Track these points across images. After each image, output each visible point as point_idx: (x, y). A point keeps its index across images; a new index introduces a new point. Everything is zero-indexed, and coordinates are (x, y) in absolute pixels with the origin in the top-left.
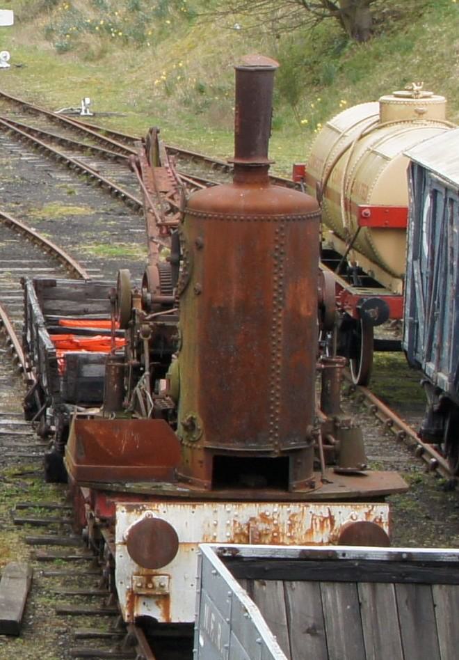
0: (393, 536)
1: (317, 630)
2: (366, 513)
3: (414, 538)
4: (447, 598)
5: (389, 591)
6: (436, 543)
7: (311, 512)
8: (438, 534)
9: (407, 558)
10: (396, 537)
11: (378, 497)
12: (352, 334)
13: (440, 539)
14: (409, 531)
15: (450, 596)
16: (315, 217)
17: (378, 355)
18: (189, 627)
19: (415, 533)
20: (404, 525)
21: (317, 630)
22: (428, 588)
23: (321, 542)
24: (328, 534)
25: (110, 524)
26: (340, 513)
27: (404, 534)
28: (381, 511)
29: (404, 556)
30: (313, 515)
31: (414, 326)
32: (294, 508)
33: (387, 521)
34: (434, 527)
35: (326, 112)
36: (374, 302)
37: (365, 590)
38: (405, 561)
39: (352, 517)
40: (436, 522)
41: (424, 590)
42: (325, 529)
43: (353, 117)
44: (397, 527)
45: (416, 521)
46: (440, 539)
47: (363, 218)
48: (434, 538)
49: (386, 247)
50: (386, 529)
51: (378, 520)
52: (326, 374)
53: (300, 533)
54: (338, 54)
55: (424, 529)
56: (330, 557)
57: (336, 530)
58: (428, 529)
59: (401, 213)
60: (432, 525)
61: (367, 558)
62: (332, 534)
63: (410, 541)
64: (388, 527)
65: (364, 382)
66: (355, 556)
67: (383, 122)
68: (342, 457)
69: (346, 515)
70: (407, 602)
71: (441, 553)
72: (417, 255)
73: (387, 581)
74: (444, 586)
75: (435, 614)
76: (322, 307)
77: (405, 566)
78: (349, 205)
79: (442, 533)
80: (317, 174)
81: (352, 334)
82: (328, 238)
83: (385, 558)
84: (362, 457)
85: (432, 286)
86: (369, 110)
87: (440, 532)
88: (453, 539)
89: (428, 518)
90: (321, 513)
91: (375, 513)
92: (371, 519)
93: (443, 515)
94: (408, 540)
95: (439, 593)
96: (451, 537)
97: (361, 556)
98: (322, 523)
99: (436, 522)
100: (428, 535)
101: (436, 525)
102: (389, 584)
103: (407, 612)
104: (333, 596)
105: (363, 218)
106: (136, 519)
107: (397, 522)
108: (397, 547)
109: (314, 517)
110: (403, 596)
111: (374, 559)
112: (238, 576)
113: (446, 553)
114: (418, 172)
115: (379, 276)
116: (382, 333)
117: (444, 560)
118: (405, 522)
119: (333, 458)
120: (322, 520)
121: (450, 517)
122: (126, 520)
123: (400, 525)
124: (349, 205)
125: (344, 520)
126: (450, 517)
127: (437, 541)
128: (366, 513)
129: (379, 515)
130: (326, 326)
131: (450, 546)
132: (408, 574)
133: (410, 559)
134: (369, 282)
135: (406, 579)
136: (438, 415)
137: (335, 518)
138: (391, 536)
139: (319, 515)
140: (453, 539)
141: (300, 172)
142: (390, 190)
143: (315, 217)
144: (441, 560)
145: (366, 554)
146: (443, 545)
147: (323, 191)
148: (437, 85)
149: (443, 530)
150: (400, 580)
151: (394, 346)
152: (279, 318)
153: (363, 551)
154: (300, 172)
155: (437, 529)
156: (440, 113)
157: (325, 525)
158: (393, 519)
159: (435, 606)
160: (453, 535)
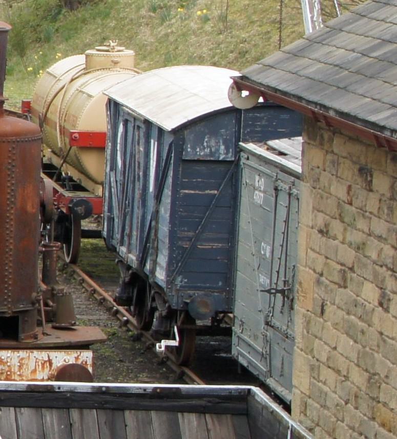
0: (96, 374)
2: (75, 358)
3: (111, 376)
4: (135, 420)
5: (92, 415)
6: (127, 380)
7: (35, 357)
8: (129, 373)
9: (106, 391)
10: (97, 375)
11: (84, 346)
12: (65, 226)
13: (130, 376)
14: (107, 371)
15: (137, 418)
16: (38, 139)
17: (85, 241)
19: (111, 372)
20: (104, 366)
22: (121, 413)
23: (42, 379)
24: (47, 373)
26: (56, 357)
27: (103, 373)
28: (87, 356)
29: (104, 389)
30: (37, 359)
31: (111, 220)
32: (22, 354)
33: (91, 363)
34: (125, 367)
35: (46, 63)
36: (82, 202)
37: (75, 414)
38: (104, 393)
39: (65, 361)
40: (127, 364)
41: (118, 414)
42: (45, 369)
43: (66, 66)
44: (98, 368)
45: (112, 363)
46: (130, 376)
47: (73, 140)
48: (126, 376)
49: (91, 162)
50: (90, 369)
51: (84, 363)
52: (46, 255)
53: (27, 372)
54: (54, 19)
55: (118, 369)
56: (49, 390)
57: (53, 370)
58: (121, 369)
59: (103, 135)
60: (124, 366)
61: (76, 391)
62: (50, 373)
63: (108, 378)
64: (91, 368)
65: (74, 261)
66: (67, 389)
67: (88, 69)
68: (57, 316)
69: (61, 359)
70: (105, 423)
71: (131, 387)
72: (113, 167)
73: (91, 408)
74: (133, 411)
75: (126, 431)
76: (43, 206)
77: (104, 397)
78: (63, 131)
79: (131, 373)
80: (39, 108)
81: (65, 226)
82: (47, 155)
83: (90, 391)
84: (72, 316)
85: (124, 191)
86: (78, 60)
87: (130, 371)
88: (139, 376)
89: (121, 361)
90: (42, 357)
91: (82, 357)
92: (79, 362)
93: (132, 359)
94: (107, 377)
95: (129, 417)
96: (138, 375)
97: (72, 389)
98: (43, 365)
99: (127, 364)
100: (121, 374)
101: (127, 367)
102: (92, 410)
103: (106, 430)
104: (51, 418)
105: (73, 140)
107: (98, 364)
108: (98, 382)
109: (37, 361)
110: (103, 418)
111: (82, 391)
113: (135, 387)
114: (114, 106)
115: (85, 183)
116: (87, 224)
117: (133, 392)
118: (105, 364)
119: (51, 317)
120: (43, 362)
121: (137, 360)
123: (101, 367)
124: (63, 131)
125: (59, 363)
126: (137, 360)
127: (128, 378)
128: (75, 358)
129: (85, 358)
130: (46, 220)
131: (137, 382)
132: (106, 402)
133: (108, 391)
134: (78, 187)
135: (105, 406)
136: (128, 285)
137: (53, 361)
138: (94, 374)
139: (41, 359)
140: (139, 376)
141: (27, 106)
142: (93, 119)
143: (38, 139)
144: (130, 392)
145: (75, 387)
146: (132, 381)
147: (44, 120)
148: (128, 42)
149: (132, 370)
150: (100, 407)
151: (96, 234)
152: (12, 214)
153: (74, 386)
154: (27, 106)
155: (128, 369)
156: (130, 62)
157: (45, 367)
158: (95, 362)
159: (126, 426)
160: (139, 373)
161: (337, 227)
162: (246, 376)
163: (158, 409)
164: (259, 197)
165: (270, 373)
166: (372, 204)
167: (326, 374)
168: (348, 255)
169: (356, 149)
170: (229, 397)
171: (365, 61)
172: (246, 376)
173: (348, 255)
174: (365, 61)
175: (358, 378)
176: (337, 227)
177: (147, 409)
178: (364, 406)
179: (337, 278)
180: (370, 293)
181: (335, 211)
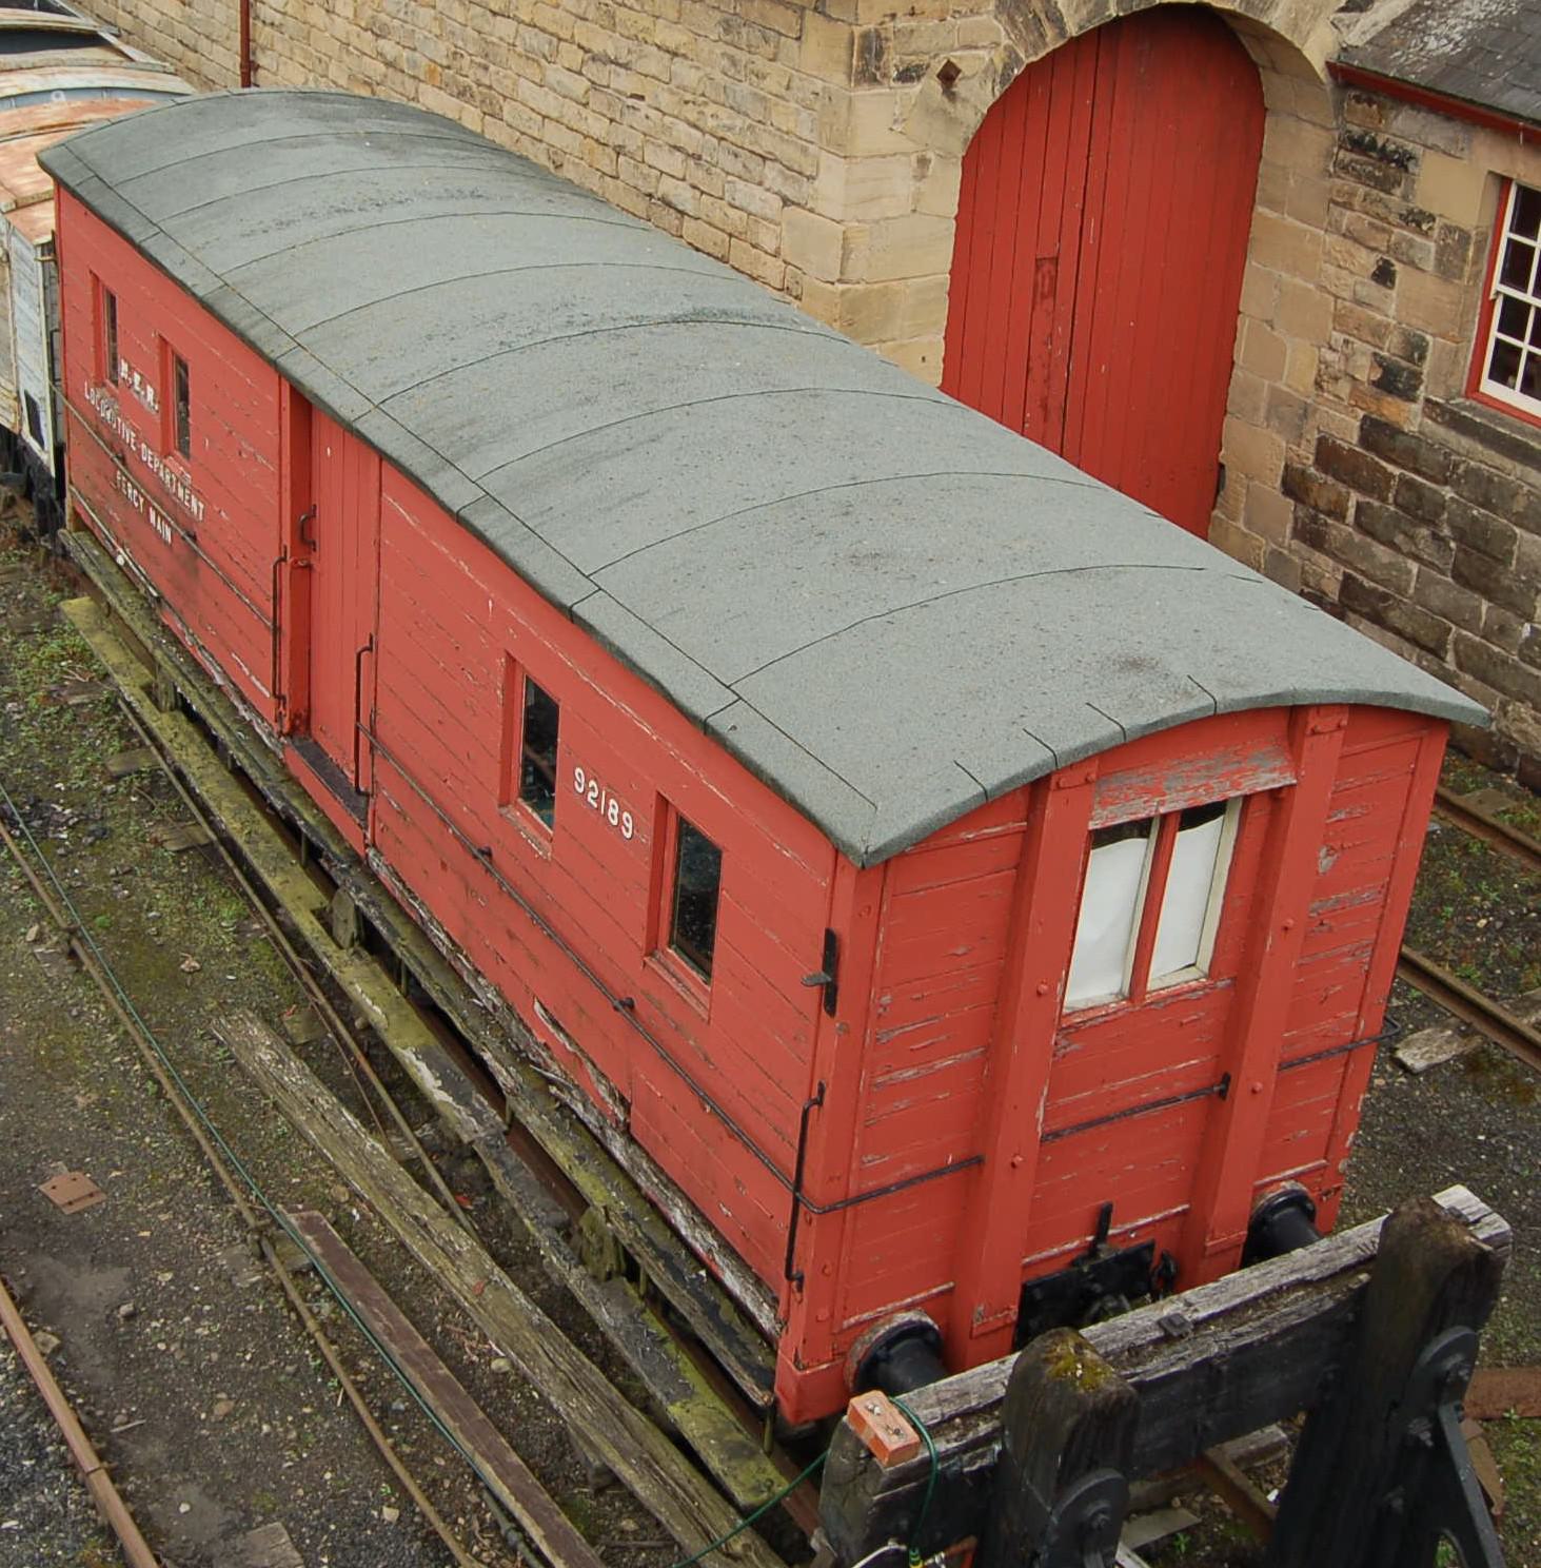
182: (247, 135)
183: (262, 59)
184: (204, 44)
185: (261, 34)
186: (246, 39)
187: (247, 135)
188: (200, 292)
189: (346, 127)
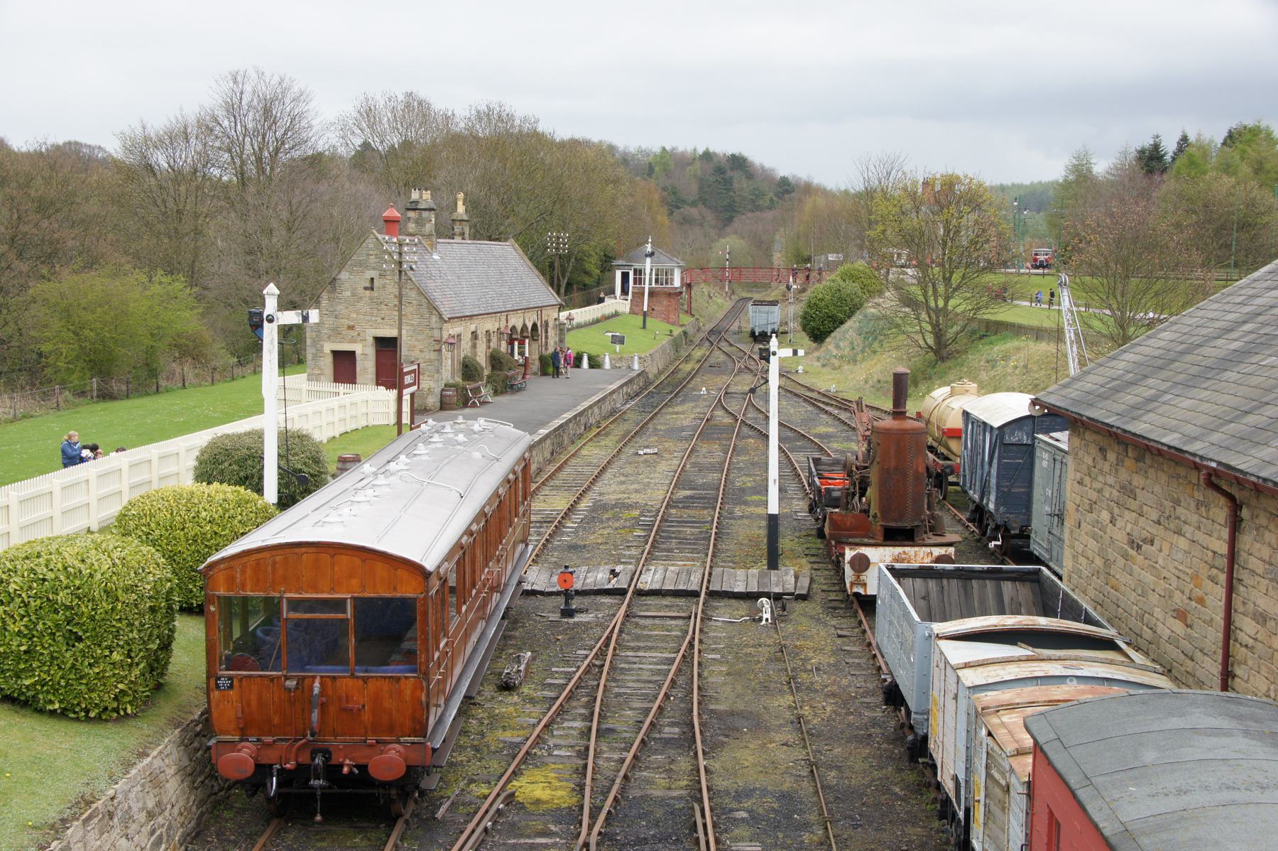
1: (926, 597)
5: (954, 582)
11: (950, 545)
12: (940, 479)
16: (925, 432)
17: (950, 488)
18: (874, 596)
21: (926, 597)
23: (927, 562)
25: (843, 555)
28: (951, 550)
31: (965, 476)
32: (916, 549)
35: (929, 391)
36: (949, 466)
37: (945, 581)
43: (940, 393)
47: (944, 433)
49: (953, 445)
52: (929, 495)
53: (919, 559)
54: (934, 367)
56: (931, 568)
59: (960, 430)
65: (944, 498)
67: (952, 394)
68: (936, 529)
69: (937, 551)
72: (966, 448)
76: (927, 468)
78: (938, 428)
80: (926, 415)
81: (940, 479)
82: (930, 441)
84: (943, 528)
85: (972, 460)
86: (947, 389)
103: (962, 590)
104: (932, 584)
105: (944, 433)
106: (853, 553)
112: (894, 576)
115: (951, 456)
116: (951, 479)
119: (932, 529)
122: (849, 554)
124: (938, 428)
130: (929, 476)
134: (947, 458)
136: (973, 512)
141: (919, 414)
142: (955, 422)
143: (925, 432)
147: (928, 422)
148: (974, 379)
150: (959, 578)
151: (956, 484)
152: (911, 472)
154: (919, 414)
156: (975, 391)
161: (1087, 480)
162: (1038, 561)
163: (990, 579)
164: (1045, 464)
165: (1051, 559)
166: (1106, 467)
167: (1081, 559)
168: (1094, 495)
169: (1098, 437)
170: (1029, 572)
171: (1103, 390)
172: (1038, 561)
173: (1094, 495)
174: (1103, 390)
175: (1099, 562)
176: (1087, 480)
177: (984, 579)
178: (1102, 577)
179: (1087, 507)
180: (1105, 516)
181: (1086, 471)
182: (1176, 722)
183: (1239, 671)
184: (1198, 655)
185: (1238, 652)
186: (1227, 655)
187: (1176, 722)
188: (1107, 832)
189: (1254, 726)
